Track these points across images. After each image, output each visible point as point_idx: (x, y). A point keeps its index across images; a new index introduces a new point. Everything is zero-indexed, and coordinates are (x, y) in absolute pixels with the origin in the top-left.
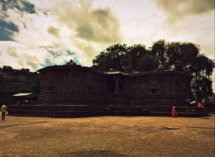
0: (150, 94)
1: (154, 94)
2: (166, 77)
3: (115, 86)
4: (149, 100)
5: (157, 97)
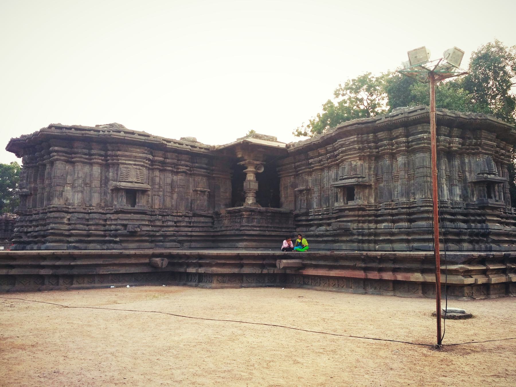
2: (391, 139)
3: (245, 184)
5: (360, 213)
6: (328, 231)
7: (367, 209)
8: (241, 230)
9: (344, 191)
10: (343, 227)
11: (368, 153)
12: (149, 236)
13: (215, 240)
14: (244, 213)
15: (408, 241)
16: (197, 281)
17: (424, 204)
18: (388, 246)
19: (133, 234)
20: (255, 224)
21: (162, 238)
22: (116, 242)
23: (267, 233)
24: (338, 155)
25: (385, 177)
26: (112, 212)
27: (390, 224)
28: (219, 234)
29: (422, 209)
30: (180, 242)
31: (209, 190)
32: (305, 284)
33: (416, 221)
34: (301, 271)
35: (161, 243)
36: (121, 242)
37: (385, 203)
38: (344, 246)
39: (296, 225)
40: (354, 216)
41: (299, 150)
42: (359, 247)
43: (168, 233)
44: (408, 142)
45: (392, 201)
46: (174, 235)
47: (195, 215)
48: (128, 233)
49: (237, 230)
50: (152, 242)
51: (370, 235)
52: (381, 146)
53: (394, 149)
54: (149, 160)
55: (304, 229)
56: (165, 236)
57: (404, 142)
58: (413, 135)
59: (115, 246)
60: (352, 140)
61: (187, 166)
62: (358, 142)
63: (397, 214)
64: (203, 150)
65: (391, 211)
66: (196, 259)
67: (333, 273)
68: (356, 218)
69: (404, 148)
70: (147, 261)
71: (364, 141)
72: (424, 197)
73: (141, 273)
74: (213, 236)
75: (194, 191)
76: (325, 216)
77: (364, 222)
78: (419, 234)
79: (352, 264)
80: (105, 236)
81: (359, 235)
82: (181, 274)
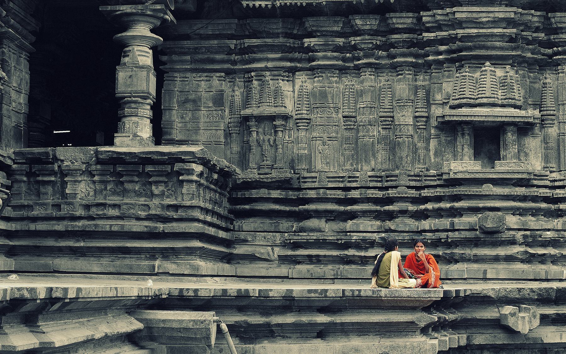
3: (121, 75)
4: (445, 223)
7: (535, 182)
14: (194, 166)
38: (492, 270)
55: (284, 224)
60: (501, 15)
76: (372, 193)
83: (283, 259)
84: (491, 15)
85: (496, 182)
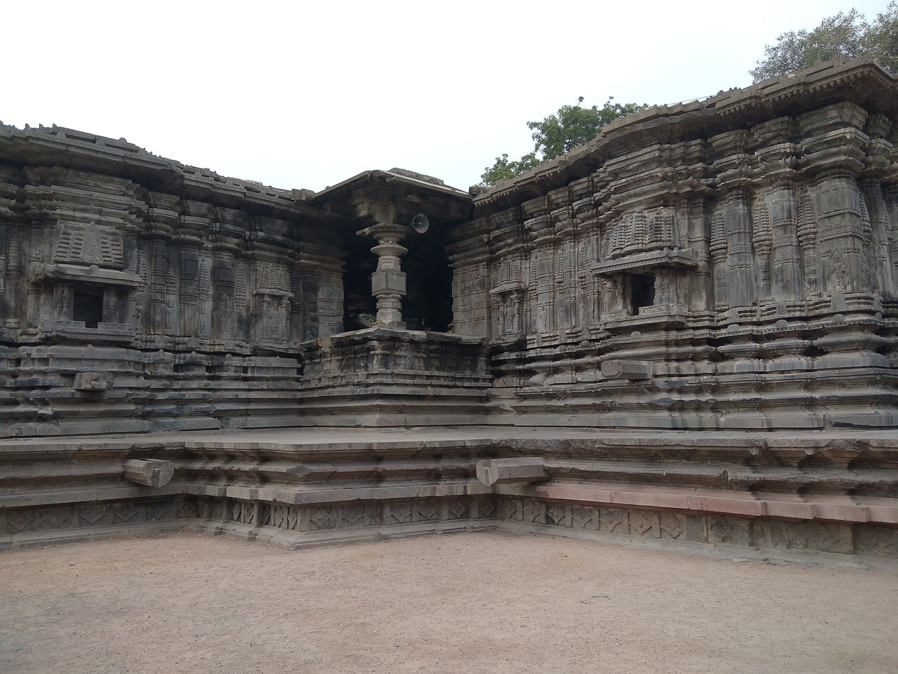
0: (617, 312)
1: (646, 314)
2: (751, 151)
3: (375, 279)
5: (673, 335)
6: (578, 382)
7: (690, 325)
8: (368, 385)
9: (624, 284)
10: (631, 371)
11: (688, 189)
12: (138, 402)
13: (302, 408)
14: (375, 343)
15: (810, 404)
16: (255, 518)
17: (851, 308)
18: (754, 418)
19: (92, 396)
20: (400, 370)
21: (174, 407)
22: (42, 418)
23: (430, 391)
24: (606, 198)
25: (733, 244)
26: (34, 339)
27: (756, 362)
28: (316, 394)
29: (848, 319)
30: (219, 415)
31: (292, 295)
32: (550, 521)
33: (826, 353)
34: (541, 488)
35: (172, 420)
36: (57, 417)
37: (738, 309)
38: (631, 418)
39: (492, 372)
40: (656, 343)
41: (502, 197)
42: (674, 421)
43: (189, 395)
44: (798, 155)
45: (754, 304)
46: (204, 400)
47: (256, 352)
48: (78, 395)
49: (359, 384)
50: (145, 416)
51: (699, 390)
52: (720, 171)
53: (758, 175)
54: (139, 213)
56: (181, 402)
57: (787, 155)
58: (809, 134)
59: (39, 427)
60: (647, 157)
61: (237, 236)
62: (659, 161)
63: (770, 337)
64: (275, 199)
65: (755, 328)
66: (253, 459)
67: (648, 496)
68: (662, 349)
69: (788, 170)
70: (116, 468)
71: (677, 160)
72: (849, 288)
73: (99, 503)
74: (301, 401)
75: (254, 296)
77: (680, 359)
78: (843, 385)
79: (711, 471)
80: (15, 403)
81: (670, 391)
82: (211, 500)
83: (520, 410)
84: (638, 159)
85: (643, 328)
